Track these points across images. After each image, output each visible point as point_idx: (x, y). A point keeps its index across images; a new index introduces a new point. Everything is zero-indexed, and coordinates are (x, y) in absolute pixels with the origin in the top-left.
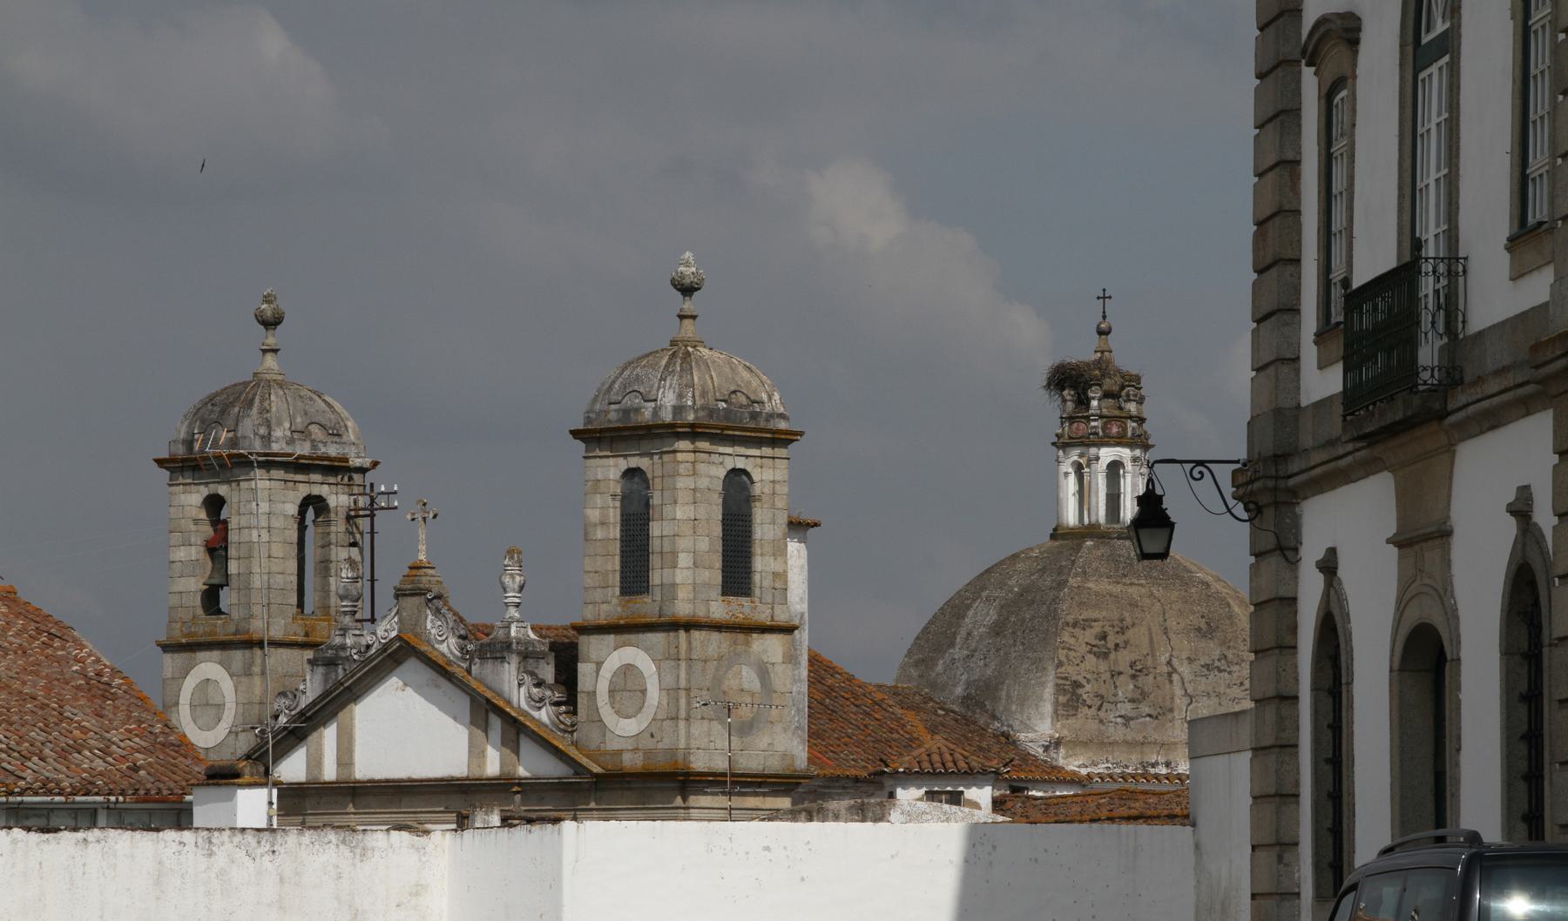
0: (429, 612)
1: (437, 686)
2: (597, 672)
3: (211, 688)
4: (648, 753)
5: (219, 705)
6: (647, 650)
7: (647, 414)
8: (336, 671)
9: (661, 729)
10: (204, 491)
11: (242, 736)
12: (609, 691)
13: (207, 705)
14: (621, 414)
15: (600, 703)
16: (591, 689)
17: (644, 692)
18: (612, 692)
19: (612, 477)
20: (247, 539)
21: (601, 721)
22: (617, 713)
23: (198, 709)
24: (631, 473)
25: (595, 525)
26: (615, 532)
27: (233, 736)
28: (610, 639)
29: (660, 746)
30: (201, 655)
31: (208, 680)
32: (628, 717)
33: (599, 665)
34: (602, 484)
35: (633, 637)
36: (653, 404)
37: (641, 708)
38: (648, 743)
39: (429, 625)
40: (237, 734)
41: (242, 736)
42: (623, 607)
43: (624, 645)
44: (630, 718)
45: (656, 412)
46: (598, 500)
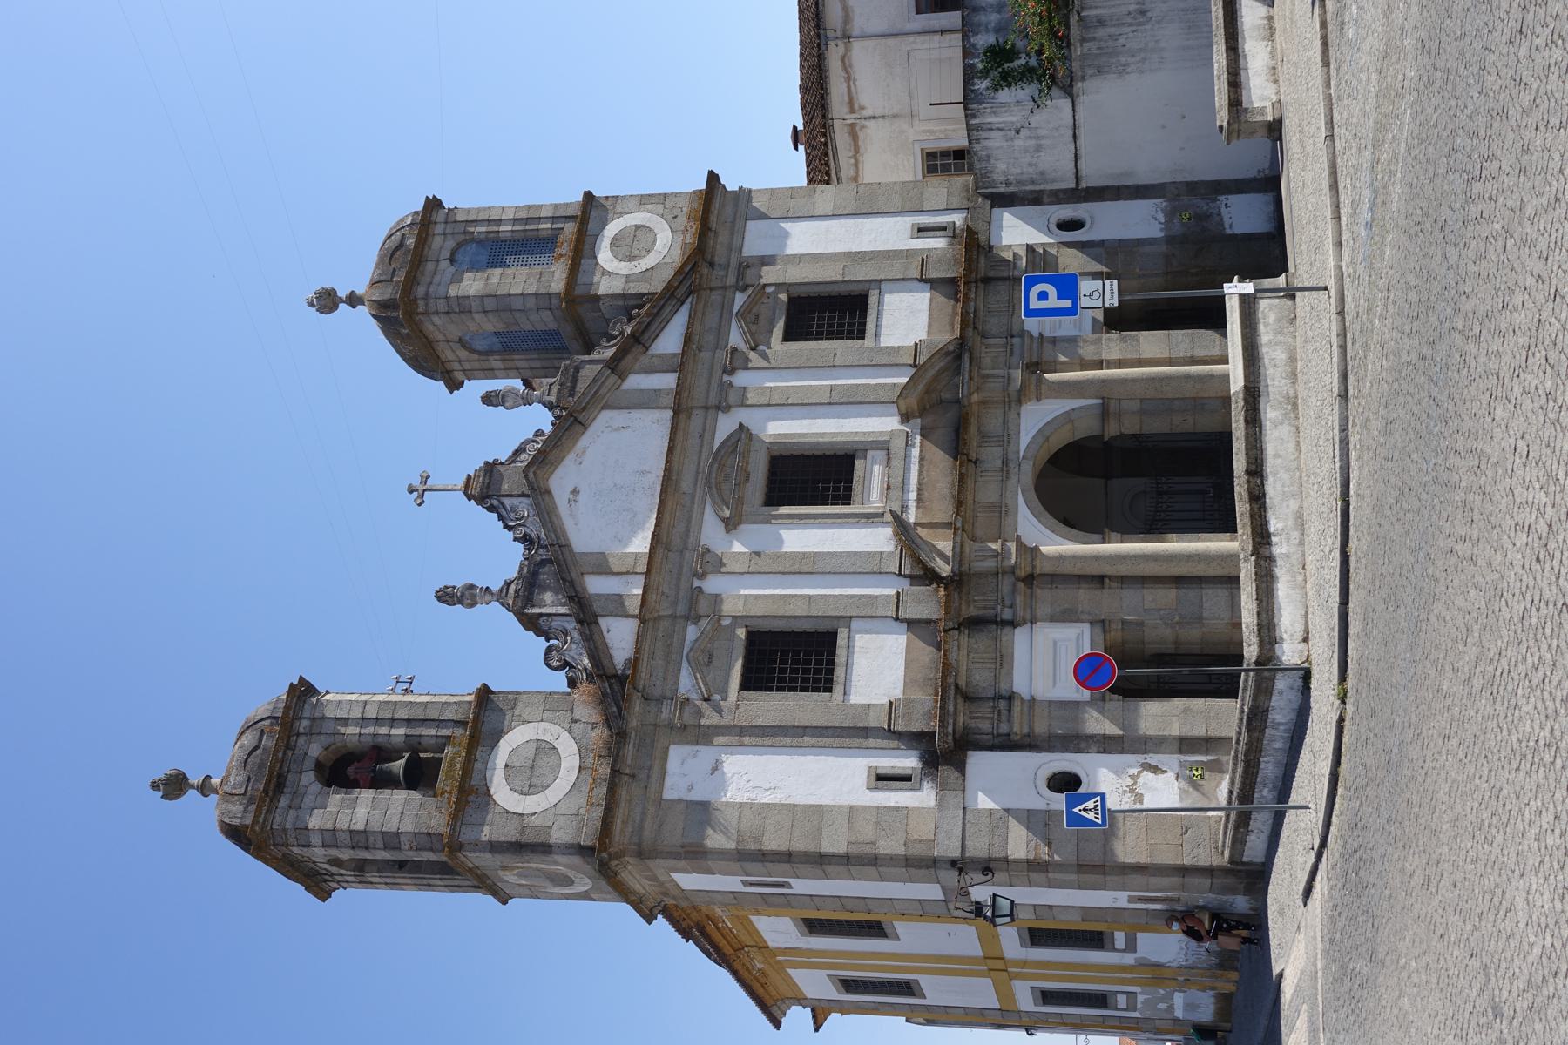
5: (537, 749)
10: (308, 778)
13: (532, 767)
15: (639, 270)
17: (637, 227)
18: (631, 259)
20: (376, 708)
21: (652, 268)
22: (649, 251)
23: (534, 780)
25: (486, 284)
29: (685, 209)
31: (506, 766)
32: (654, 242)
35: (588, 240)
37: (650, 230)
40: (574, 721)
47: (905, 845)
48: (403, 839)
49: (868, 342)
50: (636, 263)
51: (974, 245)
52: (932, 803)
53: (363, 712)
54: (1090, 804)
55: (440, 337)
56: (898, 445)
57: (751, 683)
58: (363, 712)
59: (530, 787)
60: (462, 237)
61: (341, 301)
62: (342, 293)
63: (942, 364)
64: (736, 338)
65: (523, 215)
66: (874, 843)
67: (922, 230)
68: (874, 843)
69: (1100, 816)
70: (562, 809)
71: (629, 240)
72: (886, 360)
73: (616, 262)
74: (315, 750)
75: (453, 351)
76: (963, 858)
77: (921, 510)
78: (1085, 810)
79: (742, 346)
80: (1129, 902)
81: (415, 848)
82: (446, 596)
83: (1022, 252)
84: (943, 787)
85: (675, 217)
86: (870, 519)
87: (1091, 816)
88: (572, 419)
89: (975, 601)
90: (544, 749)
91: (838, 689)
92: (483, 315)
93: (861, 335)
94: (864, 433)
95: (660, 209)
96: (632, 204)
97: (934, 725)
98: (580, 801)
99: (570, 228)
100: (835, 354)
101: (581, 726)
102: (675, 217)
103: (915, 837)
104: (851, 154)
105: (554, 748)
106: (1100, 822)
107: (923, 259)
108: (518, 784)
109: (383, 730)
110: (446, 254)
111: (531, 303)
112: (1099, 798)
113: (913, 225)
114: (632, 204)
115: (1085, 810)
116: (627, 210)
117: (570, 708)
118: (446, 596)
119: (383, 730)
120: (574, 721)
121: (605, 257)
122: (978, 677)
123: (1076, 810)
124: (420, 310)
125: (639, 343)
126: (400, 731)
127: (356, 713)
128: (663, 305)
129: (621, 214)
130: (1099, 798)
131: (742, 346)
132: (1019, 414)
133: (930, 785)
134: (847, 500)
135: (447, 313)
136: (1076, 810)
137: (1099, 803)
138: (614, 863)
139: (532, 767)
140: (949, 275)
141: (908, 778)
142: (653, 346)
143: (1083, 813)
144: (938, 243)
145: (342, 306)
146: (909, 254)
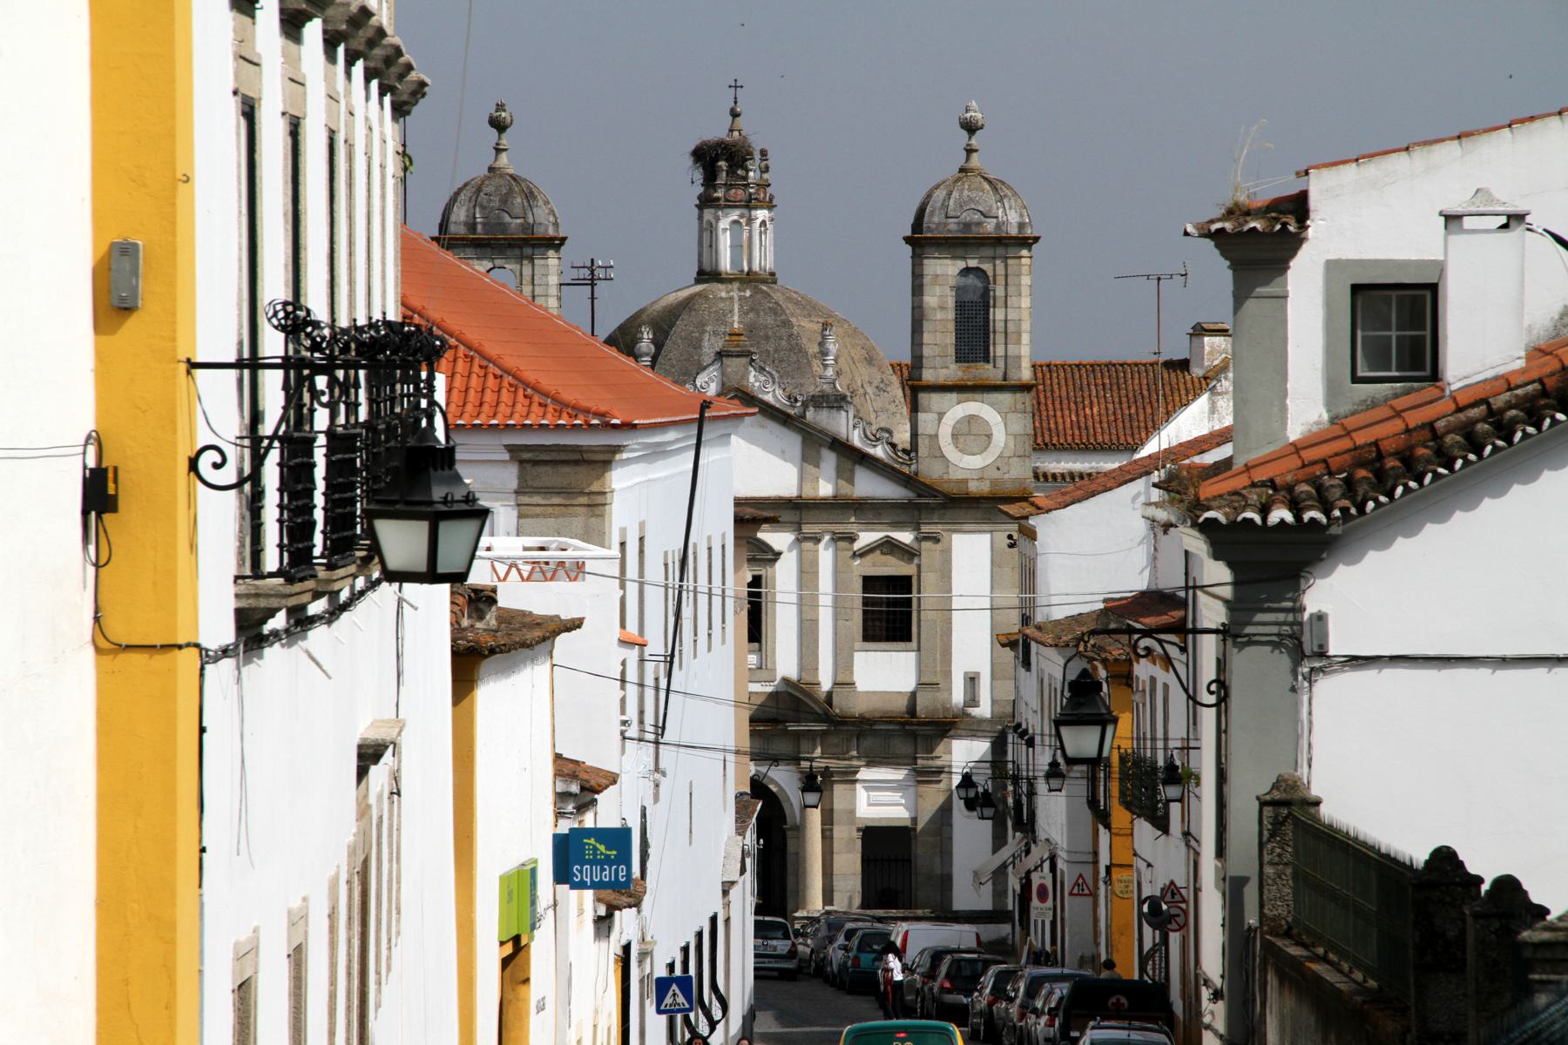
0: (751, 369)
1: (763, 427)
2: (940, 420)
4: (994, 482)
6: (992, 405)
7: (989, 227)
9: (1008, 464)
12: (953, 435)
14: (961, 226)
16: (932, 433)
17: (989, 436)
19: (950, 273)
21: (944, 456)
24: (966, 271)
25: (934, 309)
26: (951, 315)
28: (954, 396)
29: (1006, 476)
33: (941, 415)
34: (940, 278)
36: (995, 220)
37: (986, 448)
38: (996, 475)
39: (752, 379)
42: (964, 371)
43: (967, 400)
44: (974, 455)
45: (998, 226)
46: (938, 290)
49: (859, 644)
50: (950, 441)
51: (947, 726)
56: (764, 675)
64: (866, 538)
65: (1011, 327)
67: (972, 680)
72: (843, 662)
73: (953, 423)
79: (857, 546)
83: (938, 763)
85: (998, 469)
93: (867, 637)
94: (774, 649)
102: (998, 469)
110: (973, 263)
113: (978, 673)
121: (959, 409)
127: (538, 291)
131: (857, 546)
140: (918, 708)
142: (863, 469)
144: (958, 696)
146: (948, 674)
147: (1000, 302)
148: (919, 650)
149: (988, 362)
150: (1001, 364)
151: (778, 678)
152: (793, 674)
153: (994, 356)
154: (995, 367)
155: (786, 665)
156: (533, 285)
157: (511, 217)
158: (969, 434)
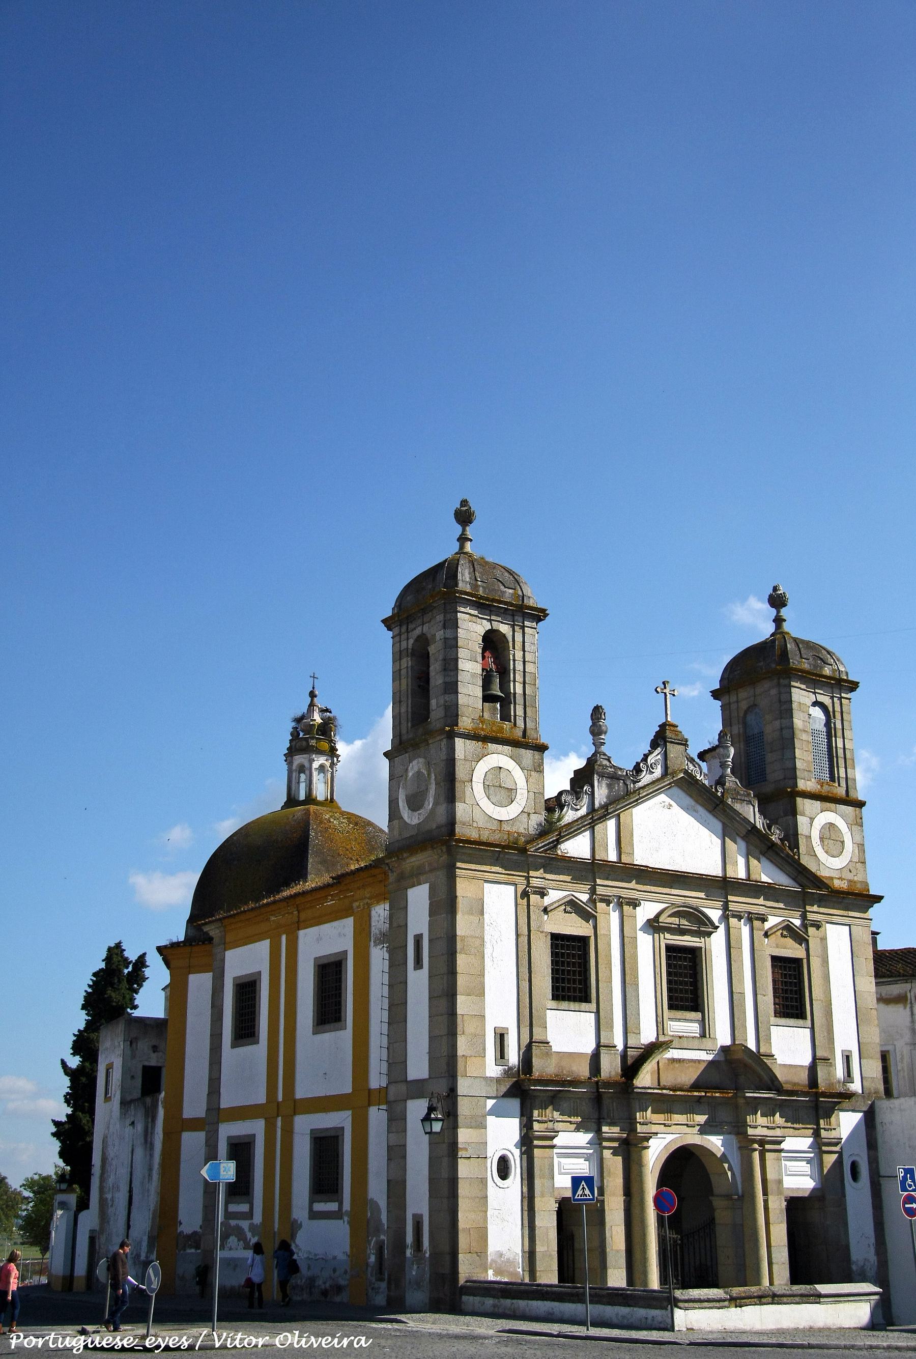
3: (503, 774)
8: (619, 784)
10: (488, 626)
11: (533, 817)
12: (820, 838)
13: (500, 787)
15: (814, 845)
17: (843, 842)
18: (822, 839)
21: (816, 855)
22: (827, 852)
25: (801, 730)
27: (526, 815)
28: (818, 804)
30: (492, 746)
31: (500, 768)
32: (833, 856)
33: (812, 819)
35: (832, 806)
37: (842, 852)
38: (850, 876)
40: (529, 814)
41: (533, 817)
47: (463, 1056)
48: (453, 696)
49: (773, 1020)
50: (819, 843)
51: (843, 1098)
52: (488, 1075)
53: (529, 662)
54: (587, 1192)
55: (759, 690)
56: (707, 1043)
57: (557, 939)
58: (529, 662)
59: (488, 785)
60: (831, 709)
61: (778, 612)
62: (784, 612)
63: (765, 1076)
66: (463, 1033)
67: (847, 1059)
68: (463, 1033)
69: (579, 1197)
70: (476, 810)
71: (833, 837)
74: (504, 629)
75: (746, 699)
76: (456, 1096)
77: (667, 1062)
78: (583, 1188)
80: (414, 1216)
81: (447, 704)
82: (597, 713)
84: (498, 1080)
85: (850, 871)
86: (660, 1025)
87: (580, 1192)
88: (718, 803)
89: (612, 1103)
90: (510, 795)
91: (553, 1004)
92: (779, 728)
94: (714, 1019)
95: (856, 859)
96: (858, 839)
97: (536, 1074)
98: (481, 822)
99: (841, 791)
100: (764, 996)
101: (526, 820)
102: (850, 871)
103: (468, 1063)
104: (883, 995)
105: (512, 802)
106: (576, 1197)
107: (829, 1060)
108: (490, 776)
109: (519, 678)
111: (789, 764)
112: (591, 1197)
114: (858, 839)
115: (583, 1188)
116: (853, 834)
117: (537, 811)
118: (597, 713)
119: (519, 678)
120: (529, 814)
122: (565, 1105)
123: (583, 1183)
124: (782, 681)
125: (768, 849)
126: (519, 690)
128: (792, 865)
129: (851, 830)
130: (591, 1197)
132: (730, 1133)
133: (499, 1072)
134: (671, 1007)
135: (780, 701)
136: (583, 1183)
137: (588, 1197)
138: (444, 849)
139: (500, 787)
141: (502, 1056)
143: (581, 1187)
144: (839, 1072)
145: (773, 612)
147: (839, 733)
148: (812, 1029)
149: (834, 782)
150: (843, 783)
151: (719, 1047)
152: (728, 1042)
153: (839, 777)
154: (839, 785)
155: (723, 1037)
156: (524, 651)
157: (505, 587)
158: (829, 839)
